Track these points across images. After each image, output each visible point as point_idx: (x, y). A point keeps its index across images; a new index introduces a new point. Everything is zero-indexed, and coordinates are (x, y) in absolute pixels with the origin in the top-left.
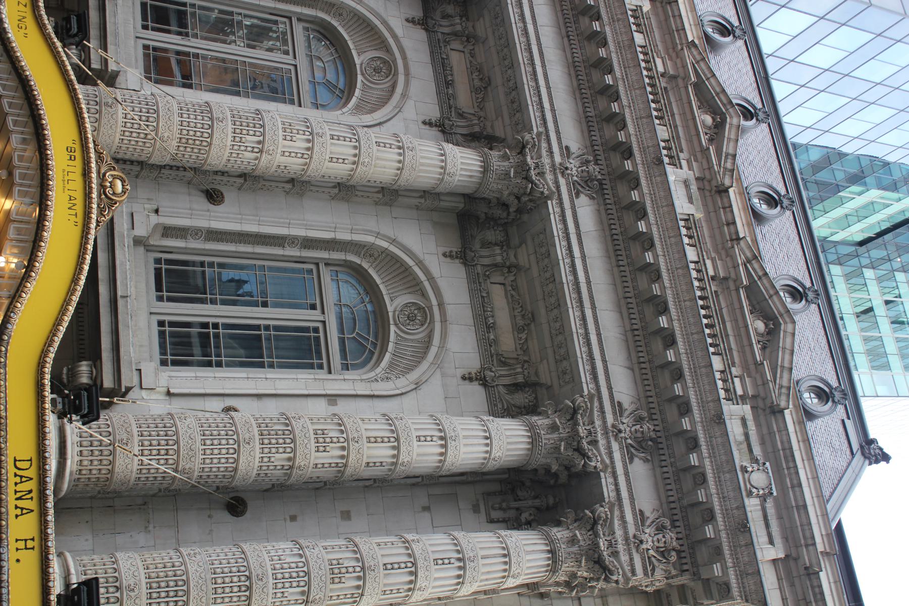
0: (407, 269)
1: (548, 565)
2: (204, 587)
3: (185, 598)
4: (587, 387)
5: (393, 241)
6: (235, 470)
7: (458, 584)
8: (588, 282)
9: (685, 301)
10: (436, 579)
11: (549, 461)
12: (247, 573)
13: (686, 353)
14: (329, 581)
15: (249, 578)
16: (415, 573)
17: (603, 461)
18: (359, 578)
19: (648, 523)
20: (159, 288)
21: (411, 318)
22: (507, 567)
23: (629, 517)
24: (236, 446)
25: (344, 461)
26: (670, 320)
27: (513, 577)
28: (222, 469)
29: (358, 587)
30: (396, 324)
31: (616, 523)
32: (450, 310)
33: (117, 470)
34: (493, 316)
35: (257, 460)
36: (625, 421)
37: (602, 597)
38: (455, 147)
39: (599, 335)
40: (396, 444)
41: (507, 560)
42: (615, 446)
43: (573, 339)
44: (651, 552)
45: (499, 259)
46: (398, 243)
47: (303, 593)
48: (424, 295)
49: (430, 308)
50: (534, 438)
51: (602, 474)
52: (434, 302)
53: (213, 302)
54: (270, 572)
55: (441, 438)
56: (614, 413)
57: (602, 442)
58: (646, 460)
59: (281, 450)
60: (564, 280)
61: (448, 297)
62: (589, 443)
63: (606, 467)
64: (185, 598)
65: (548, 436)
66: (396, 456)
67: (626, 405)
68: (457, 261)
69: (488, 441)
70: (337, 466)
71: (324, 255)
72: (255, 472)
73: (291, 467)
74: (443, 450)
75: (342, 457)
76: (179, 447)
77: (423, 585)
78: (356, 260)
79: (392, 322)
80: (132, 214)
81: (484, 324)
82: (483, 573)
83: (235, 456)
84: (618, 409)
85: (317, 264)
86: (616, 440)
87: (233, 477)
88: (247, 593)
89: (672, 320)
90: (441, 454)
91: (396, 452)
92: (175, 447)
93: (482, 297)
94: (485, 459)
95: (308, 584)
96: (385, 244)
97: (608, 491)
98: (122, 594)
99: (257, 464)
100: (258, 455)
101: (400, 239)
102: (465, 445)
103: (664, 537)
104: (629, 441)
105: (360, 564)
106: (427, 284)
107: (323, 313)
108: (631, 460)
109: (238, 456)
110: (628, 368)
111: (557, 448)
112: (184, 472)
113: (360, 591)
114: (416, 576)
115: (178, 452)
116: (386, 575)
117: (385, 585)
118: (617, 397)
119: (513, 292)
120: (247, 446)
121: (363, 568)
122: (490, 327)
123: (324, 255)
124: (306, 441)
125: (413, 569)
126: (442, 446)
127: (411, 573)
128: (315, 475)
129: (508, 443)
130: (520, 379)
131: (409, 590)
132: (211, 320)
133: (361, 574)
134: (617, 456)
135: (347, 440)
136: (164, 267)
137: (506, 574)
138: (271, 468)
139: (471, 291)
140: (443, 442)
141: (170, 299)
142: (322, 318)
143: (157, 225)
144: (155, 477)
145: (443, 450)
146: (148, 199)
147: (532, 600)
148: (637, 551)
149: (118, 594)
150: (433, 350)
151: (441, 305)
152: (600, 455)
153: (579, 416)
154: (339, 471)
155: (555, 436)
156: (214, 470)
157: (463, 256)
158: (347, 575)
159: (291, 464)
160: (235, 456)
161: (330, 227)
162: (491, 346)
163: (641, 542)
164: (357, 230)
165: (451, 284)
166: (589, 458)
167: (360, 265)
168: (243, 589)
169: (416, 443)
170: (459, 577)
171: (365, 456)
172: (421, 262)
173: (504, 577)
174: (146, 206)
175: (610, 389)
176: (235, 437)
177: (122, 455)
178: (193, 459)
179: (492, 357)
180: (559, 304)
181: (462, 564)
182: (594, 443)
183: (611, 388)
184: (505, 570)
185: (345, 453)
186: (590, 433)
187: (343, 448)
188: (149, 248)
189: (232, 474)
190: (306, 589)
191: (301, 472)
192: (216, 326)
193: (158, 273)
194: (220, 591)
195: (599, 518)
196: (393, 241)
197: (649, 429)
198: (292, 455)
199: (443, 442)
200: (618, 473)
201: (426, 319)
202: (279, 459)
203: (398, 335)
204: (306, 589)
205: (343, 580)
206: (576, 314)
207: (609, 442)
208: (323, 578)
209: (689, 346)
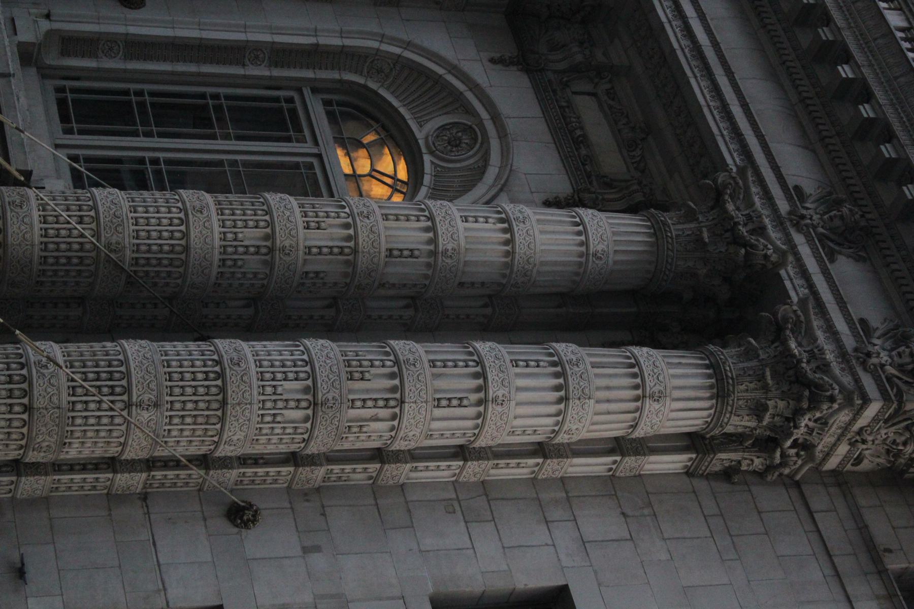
0: (438, 80)
1: (711, 387)
2: (150, 369)
3: (124, 383)
4: (732, 159)
5: (408, 45)
6: (187, 249)
7: (560, 401)
8: (715, 44)
9: (875, 39)
10: (519, 389)
11: (690, 264)
12: (215, 357)
13: (892, 105)
14: (344, 376)
15: (218, 362)
16: (483, 375)
17: (776, 249)
18: (392, 376)
19: (878, 333)
20: (64, 118)
21: (455, 143)
22: (638, 380)
23: (841, 325)
24: (182, 215)
25: (352, 244)
26: (857, 67)
27: (652, 396)
28: (166, 248)
29: (394, 389)
30: (431, 153)
31: (816, 323)
32: (511, 126)
33: (10, 240)
34: (582, 128)
35: (217, 236)
36: (808, 205)
37: (839, 485)
38: (602, 215)
39: (745, 106)
40: (429, 223)
41: (636, 370)
42: (799, 239)
43: (704, 116)
44: (890, 370)
45: (579, 58)
46: (416, 46)
47: (306, 390)
48: (469, 110)
49: (481, 124)
50: (658, 231)
51: (782, 272)
52: (484, 115)
53: (148, 134)
54: (251, 359)
55: (502, 221)
56: (789, 198)
57: (774, 234)
58: (858, 259)
59: (251, 223)
60: (676, 45)
61: (505, 108)
62: (752, 232)
63: (783, 254)
64: (124, 383)
65: (680, 227)
66: (434, 241)
67: (809, 187)
68: (515, 68)
69: (581, 228)
70: (341, 253)
71: (309, 74)
72: (217, 257)
73: (271, 250)
74: (508, 236)
75: (349, 238)
76: (97, 213)
77: (500, 393)
78: (361, 81)
79: (424, 150)
80: (13, 20)
81: (569, 140)
82: (598, 389)
83: (183, 228)
84: (796, 194)
85: (300, 91)
86: (799, 231)
87: (185, 263)
88: (219, 382)
89: (859, 67)
90: (506, 243)
91: (431, 235)
92: (92, 213)
93: (561, 107)
94: (581, 255)
95: (312, 375)
96: (398, 51)
97: (795, 290)
98: (30, 371)
99: (217, 243)
100: (217, 229)
101: (417, 41)
102: (541, 232)
103: (908, 347)
104: (821, 230)
105: (392, 358)
106: (470, 96)
107: (316, 143)
108: (832, 261)
109: (188, 227)
110: (806, 148)
111: (699, 240)
112: (108, 246)
113: (398, 396)
114: (485, 379)
115: (97, 219)
116: (436, 376)
117: (436, 391)
118: (791, 183)
119: (611, 102)
120: (199, 215)
121: (397, 362)
122: (581, 141)
123: (309, 74)
124: (288, 213)
125: (478, 369)
126: (505, 231)
127: (476, 376)
128: (308, 268)
129: (614, 233)
130: (639, 197)
131: (479, 403)
132: (147, 155)
133: (395, 369)
134: (805, 251)
135: (351, 215)
136: (70, 96)
137: (639, 392)
138: (241, 250)
139: (541, 101)
140: (506, 225)
141: (81, 132)
142: (315, 151)
143: (50, 33)
144: (69, 258)
145: (508, 236)
146: (34, 3)
147: (713, 484)
148: (865, 370)
149: (24, 372)
150: (492, 172)
151: (496, 117)
152: (772, 243)
153: (727, 197)
154: (347, 262)
155: (692, 225)
156: (154, 248)
157: (524, 60)
158: (373, 371)
159: (269, 244)
160: (183, 228)
161: (308, 30)
162: (584, 165)
163: (869, 355)
164: (349, 32)
165: (511, 97)
166: (753, 246)
167: (365, 87)
168: (212, 375)
169: (461, 225)
170: (557, 388)
171: (383, 239)
172: (455, 67)
173: (637, 399)
174: (32, 11)
175: (776, 169)
176: (180, 205)
177: (15, 220)
178: (120, 229)
179: (589, 177)
180: (680, 86)
181: (559, 369)
182: (760, 230)
183: (778, 167)
184: (636, 387)
185: (351, 232)
186: (749, 218)
187: (347, 226)
188: (45, 73)
189: (183, 256)
190: (309, 382)
191: (287, 259)
192: (155, 161)
193: (62, 104)
194: (177, 391)
195: (786, 320)
196: (408, 45)
197: (851, 210)
198: (268, 230)
199: (506, 225)
200: (811, 270)
201: (475, 140)
202: (251, 236)
203: (436, 166)
204: (309, 382)
205: (367, 375)
206: (702, 84)
207: (788, 235)
208: (335, 369)
209: (894, 94)
